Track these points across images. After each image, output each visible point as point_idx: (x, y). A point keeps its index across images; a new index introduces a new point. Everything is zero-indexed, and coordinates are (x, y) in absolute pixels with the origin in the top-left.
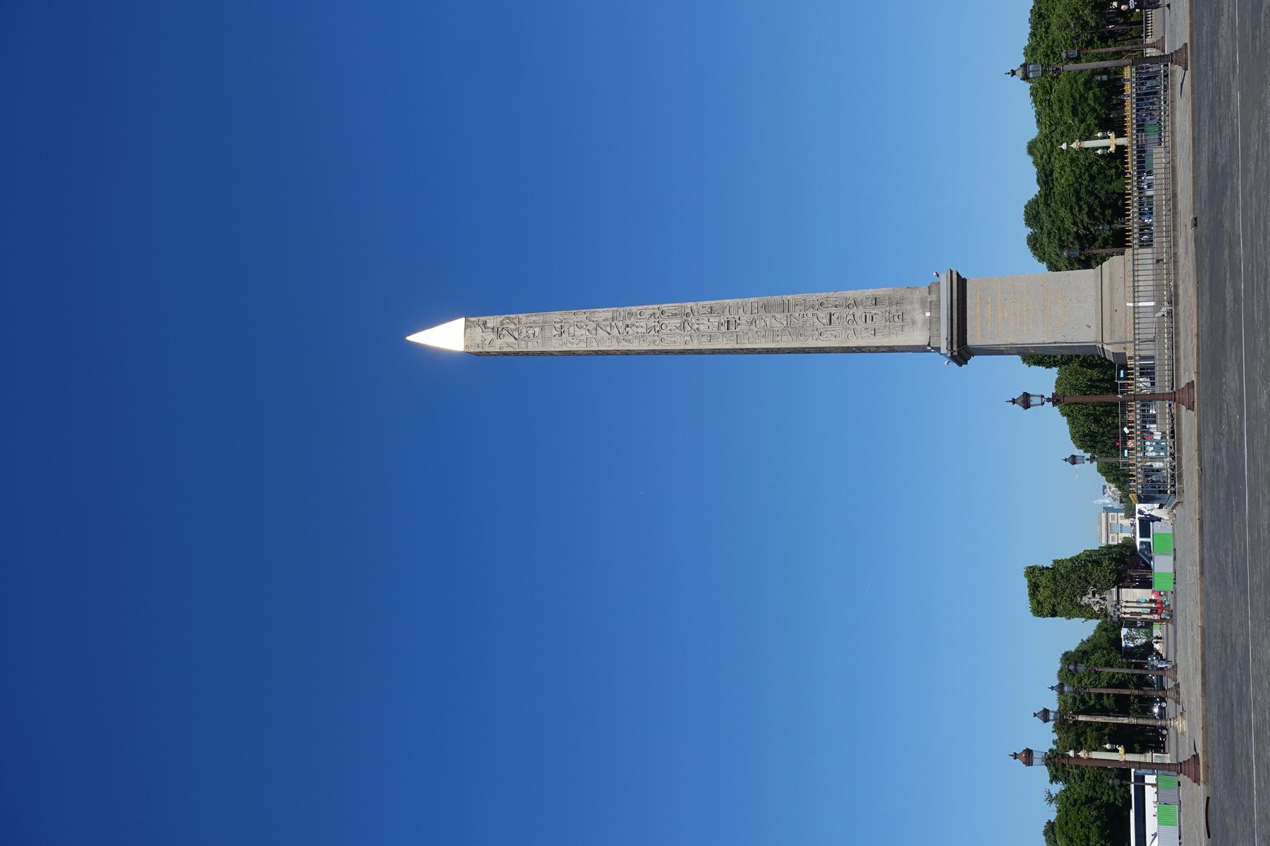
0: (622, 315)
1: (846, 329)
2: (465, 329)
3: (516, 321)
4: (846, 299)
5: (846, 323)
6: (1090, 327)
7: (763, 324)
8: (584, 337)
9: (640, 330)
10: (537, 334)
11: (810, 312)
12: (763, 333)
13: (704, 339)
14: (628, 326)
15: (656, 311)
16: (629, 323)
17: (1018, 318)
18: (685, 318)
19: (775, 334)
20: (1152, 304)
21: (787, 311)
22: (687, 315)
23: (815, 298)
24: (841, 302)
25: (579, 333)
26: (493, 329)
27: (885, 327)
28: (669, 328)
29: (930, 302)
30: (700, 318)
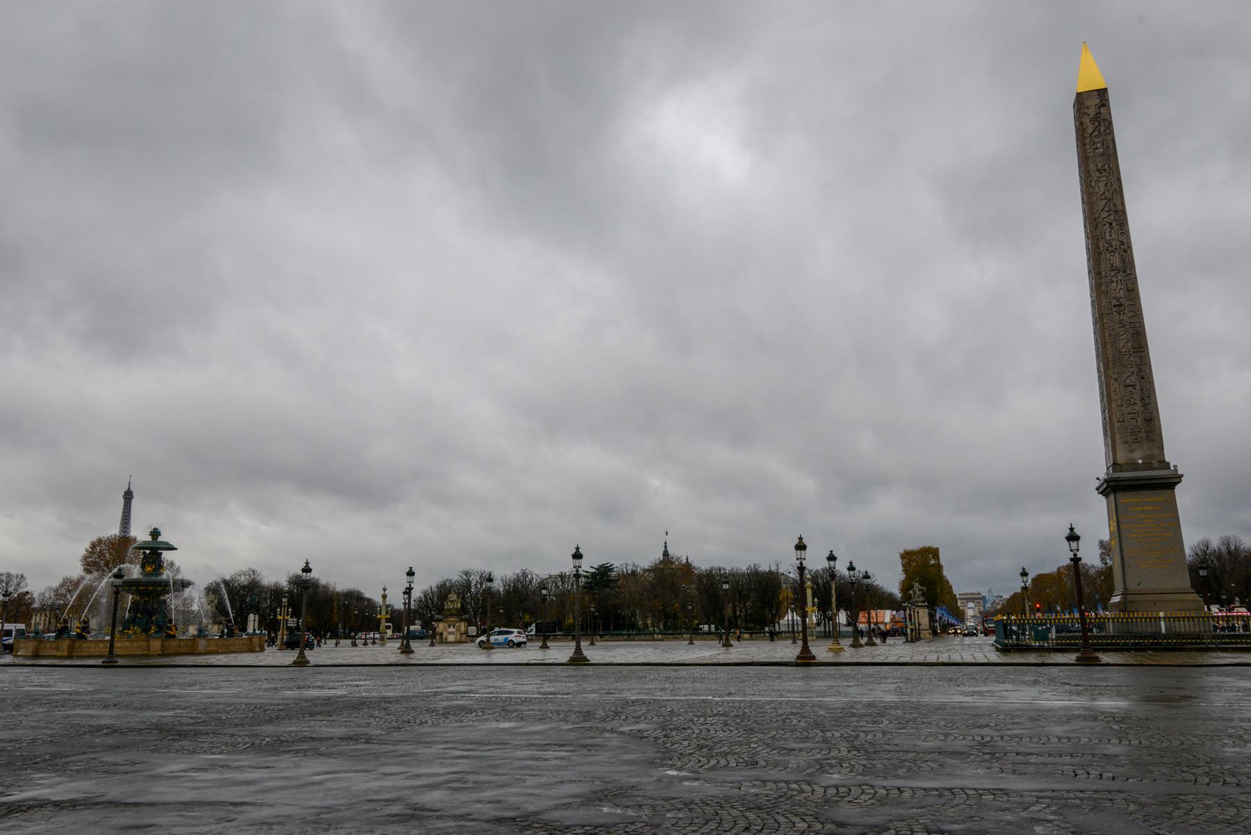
1: (1122, 399)
2: (1097, 90)
4: (1149, 397)
5: (1127, 398)
6: (1139, 584)
7: (1122, 333)
9: (1108, 234)
11: (1135, 369)
12: (1113, 334)
14: (1111, 224)
15: (1126, 245)
16: (1114, 224)
17: (1142, 531)
18: (1122, 269)
20: (1163, 631)
22: (1125, 271)
26: (1099, 113)
27: (1126, 429)
28: (1111, 258)
29: (1151, 463)
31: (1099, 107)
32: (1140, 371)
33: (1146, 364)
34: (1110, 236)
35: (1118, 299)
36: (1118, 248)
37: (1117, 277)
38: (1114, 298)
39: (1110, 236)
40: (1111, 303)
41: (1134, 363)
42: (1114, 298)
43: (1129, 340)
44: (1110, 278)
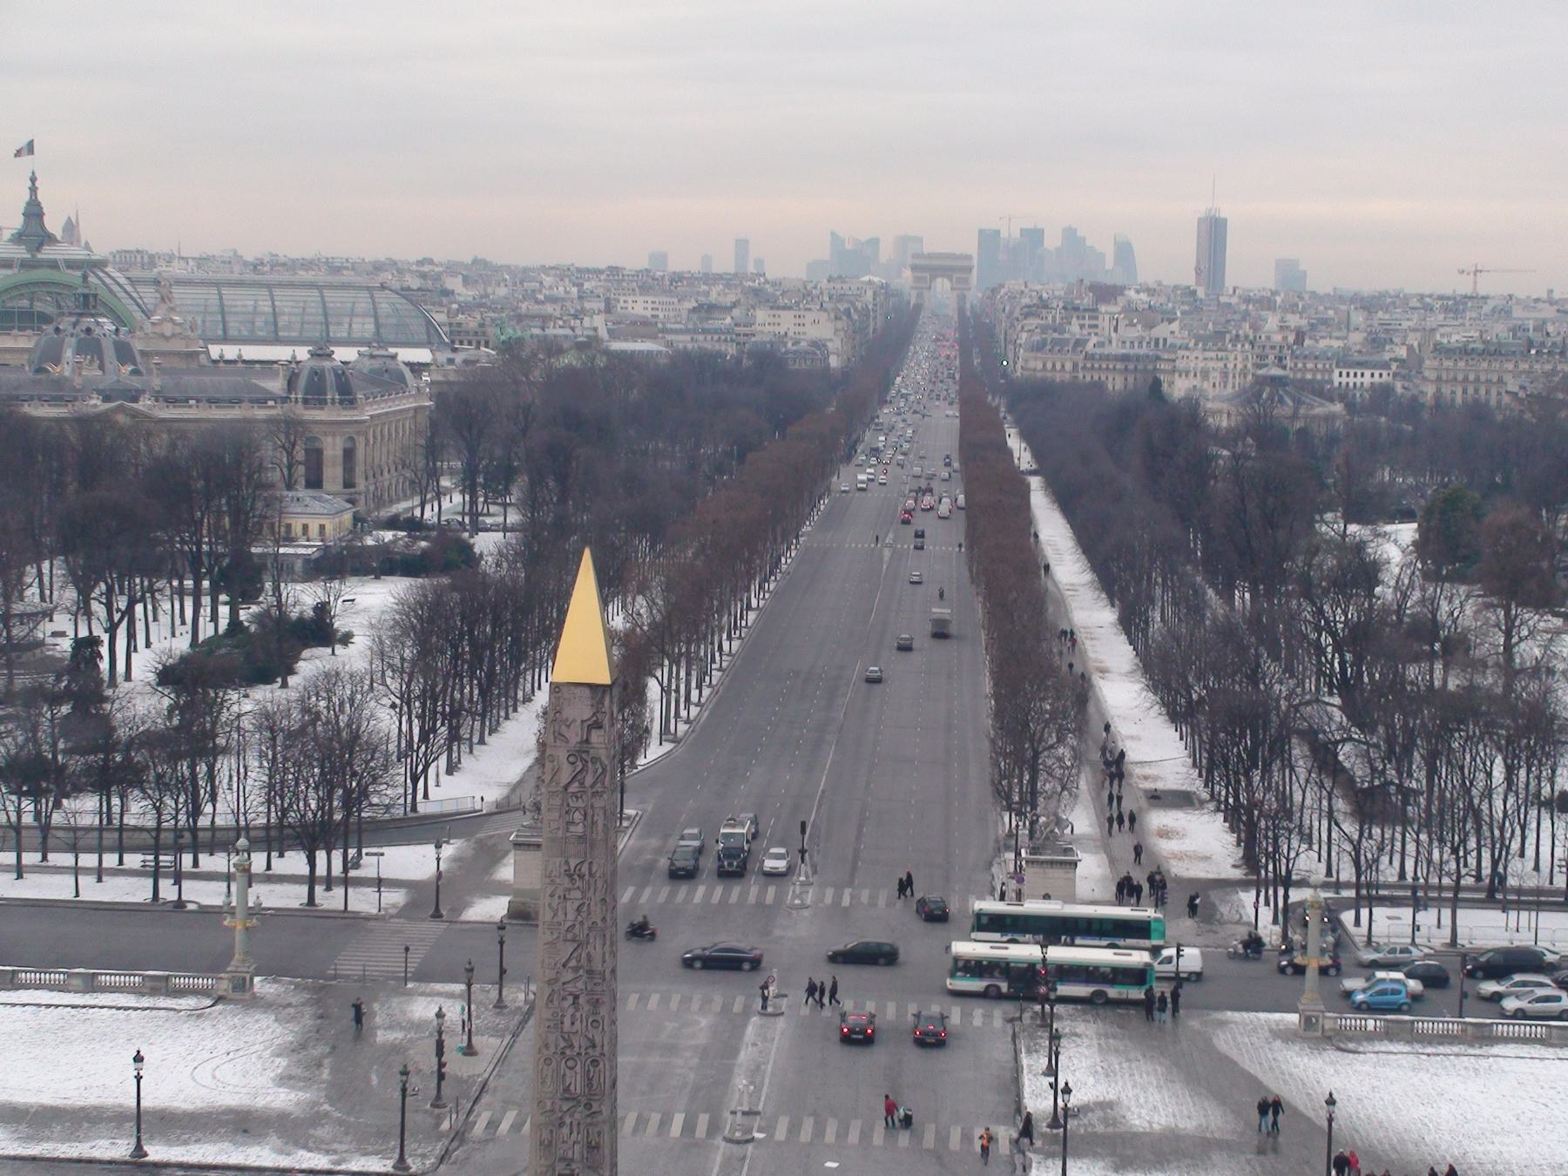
3: (598, 787)
9: (567, 1021)
10: (572, 828)
13: (546, 1135)
14: (576, 997)
15: (598, 1049)
16: (582, 1000)
18: (584, 1100)
22: (588, 1106)
25: (571, 907)
26: (587, 741)
30: (582, 1128)
31: (590, 728)
34: (573, 1024)
37: (572, 1116)
38: (563, 1159)
39: (573, 1024)
42: (563, 1159)
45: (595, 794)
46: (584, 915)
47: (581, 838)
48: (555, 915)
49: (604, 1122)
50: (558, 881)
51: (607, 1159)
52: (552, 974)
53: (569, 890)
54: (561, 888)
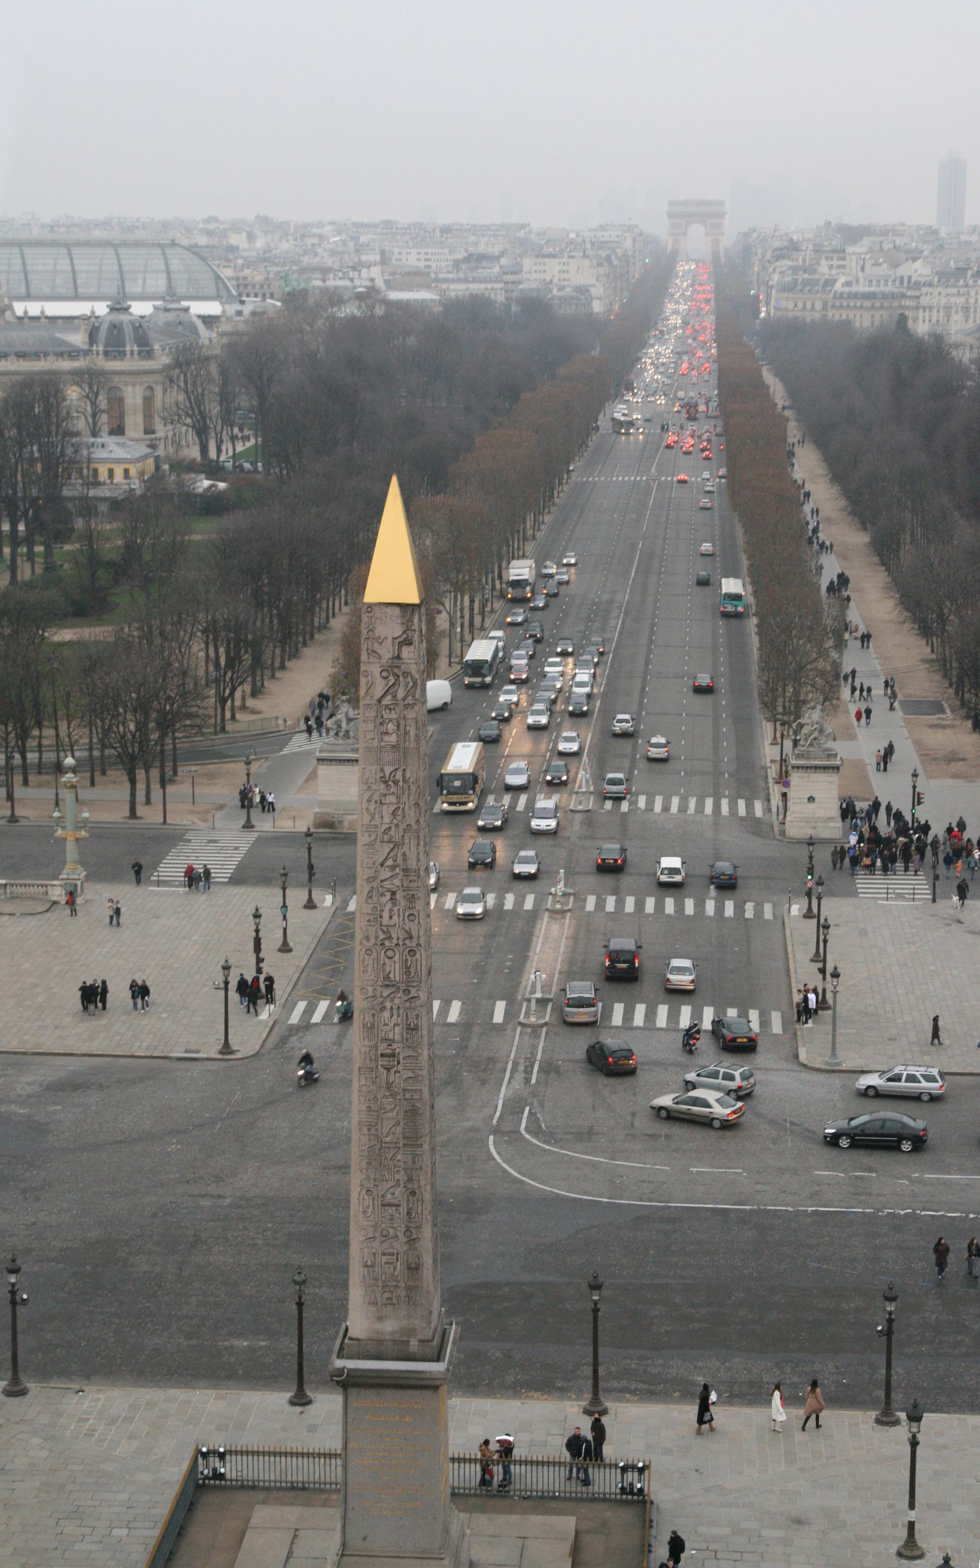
0: (414, 885)
1: (375, 1227)
3: (410, 700)
4: (419, 1228)
5: (384, 1226)
6: (364, 1539)
7: (388, 1107)
8: (377, 821)
9: (386, 915)
10: (386, 738)
11: (401, 1176)
12: (374, 1107)
13: (368, 1018)
14: (394, 893)
15: (415, 941)
16: (399, 896)
18: (403, 986)
19: (372, 1127)
21: (405, 1141)
22: (407, 992)
23: (422, 1184)
24: (416, 1219)
25: (387, 811)
26: (398, 657)
27: (376, 1279)
30: (401, 1012)
31: (401, 644)
32: (410, 1180)
33: (421, 1168)
34: (391, 917)
35: (389, 1042)
36: (401, 944)
37: (392, 1001)
38: (385, 1040)
39: (391, 917)
40: (376, 1047)
41: (402, 1165)
43: (397, 1124)
44: (381, 1000)
45: (406, 706)
46: (399, 818)
47: (394, 747)
48: (373, 818)
49: (421, 1006)
50: (374, 787)
51: (426, 1039)
52: (371, 873)
53: (385, 795)
54: (378, 793)
